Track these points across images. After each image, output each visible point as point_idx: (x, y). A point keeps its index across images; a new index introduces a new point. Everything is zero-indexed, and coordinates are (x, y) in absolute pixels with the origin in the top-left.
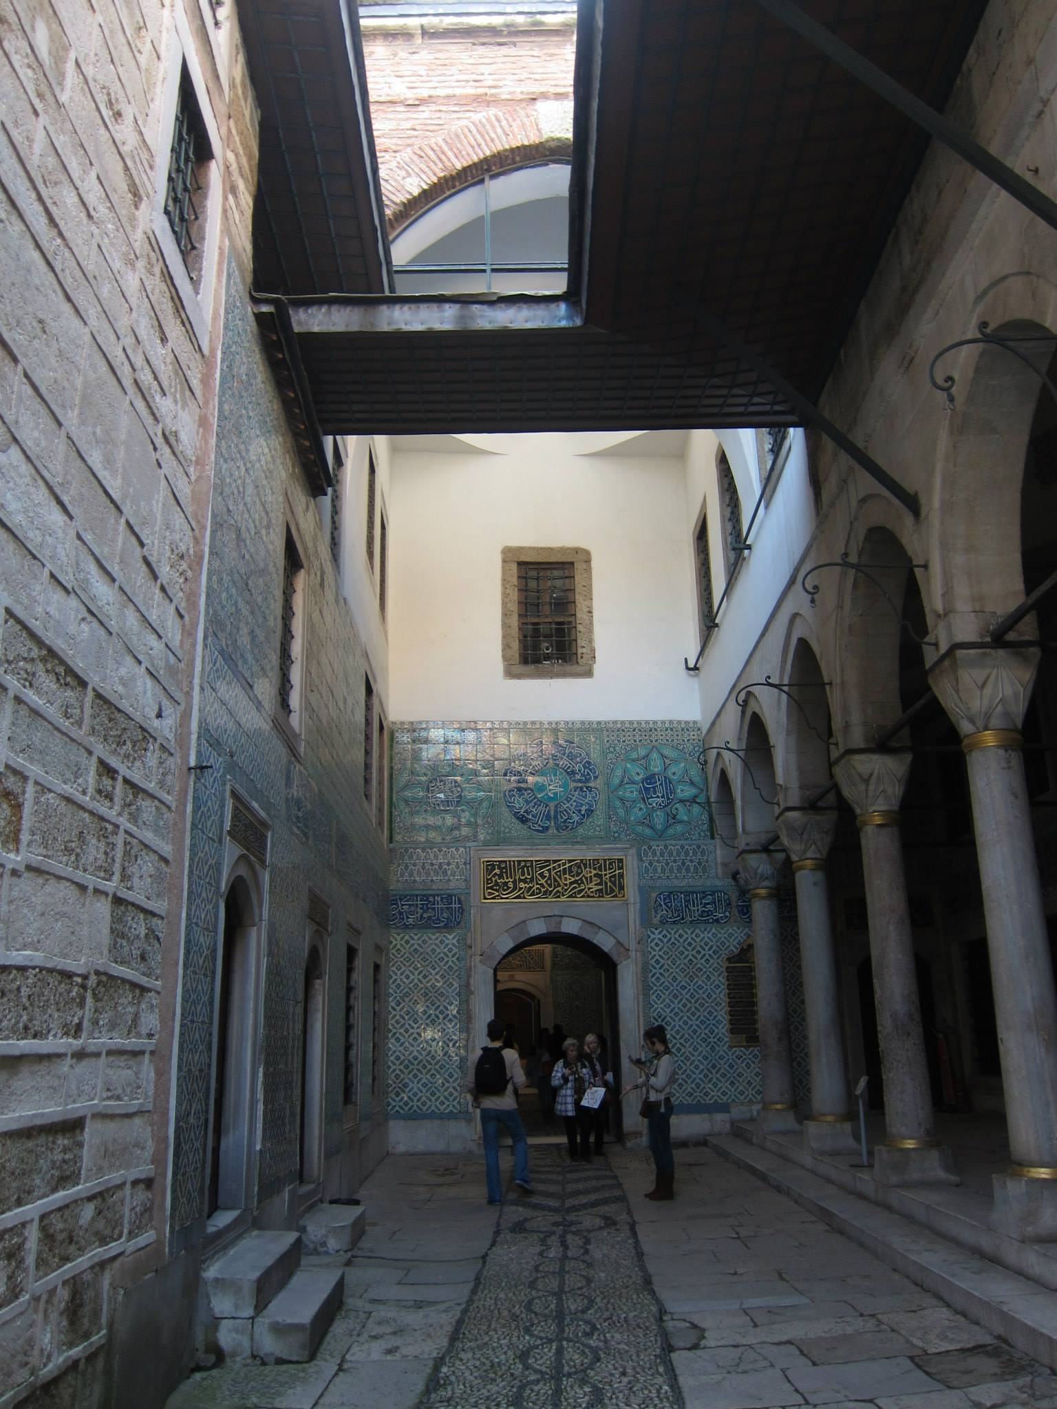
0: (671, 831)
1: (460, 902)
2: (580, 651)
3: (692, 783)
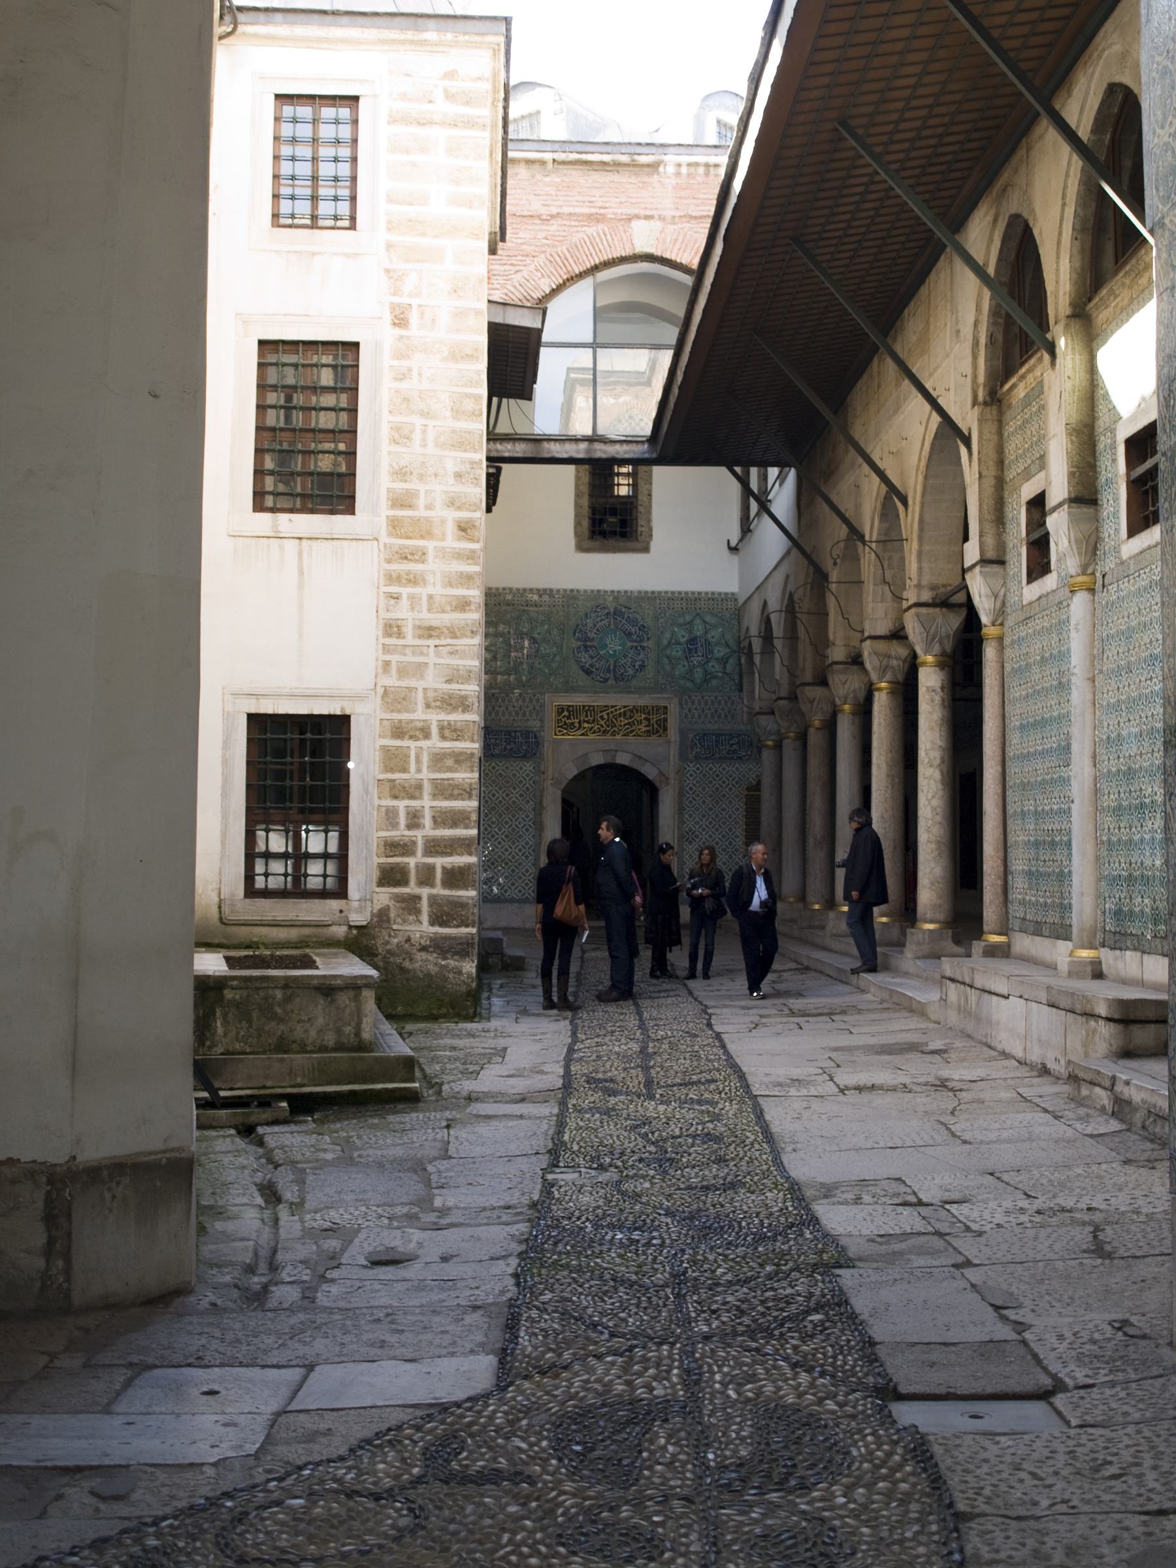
1: (536, 737)
2: (640, 529)
3: (727, 645)
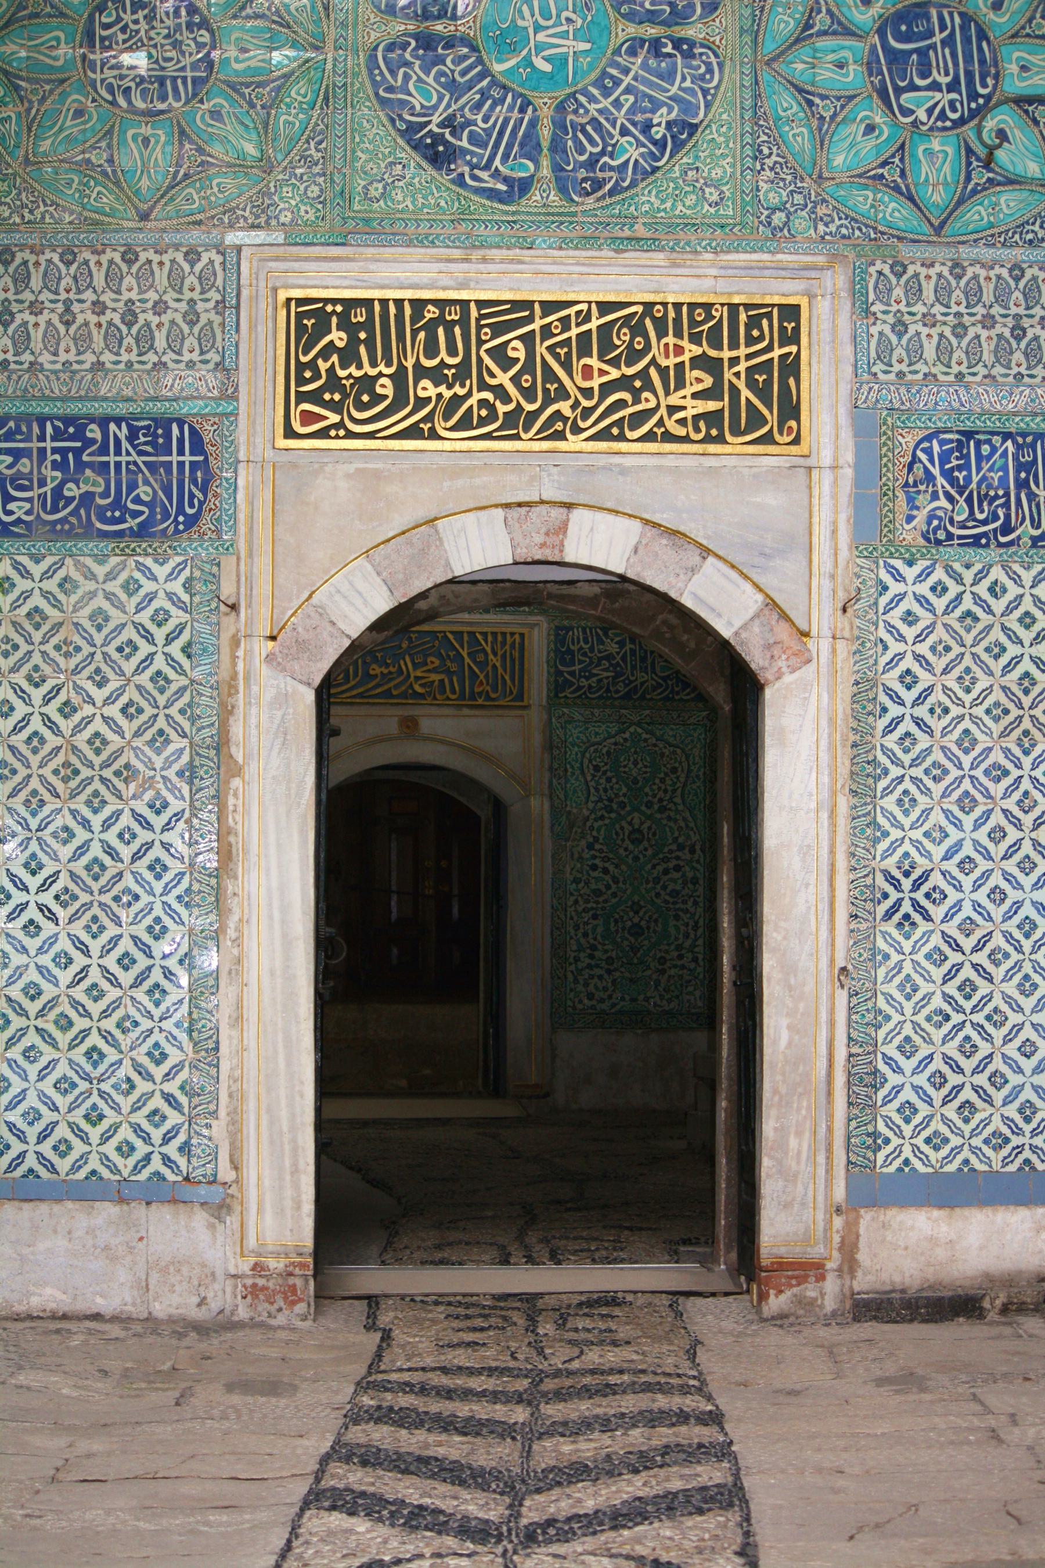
0: (977, 214)
1: (198, 445)
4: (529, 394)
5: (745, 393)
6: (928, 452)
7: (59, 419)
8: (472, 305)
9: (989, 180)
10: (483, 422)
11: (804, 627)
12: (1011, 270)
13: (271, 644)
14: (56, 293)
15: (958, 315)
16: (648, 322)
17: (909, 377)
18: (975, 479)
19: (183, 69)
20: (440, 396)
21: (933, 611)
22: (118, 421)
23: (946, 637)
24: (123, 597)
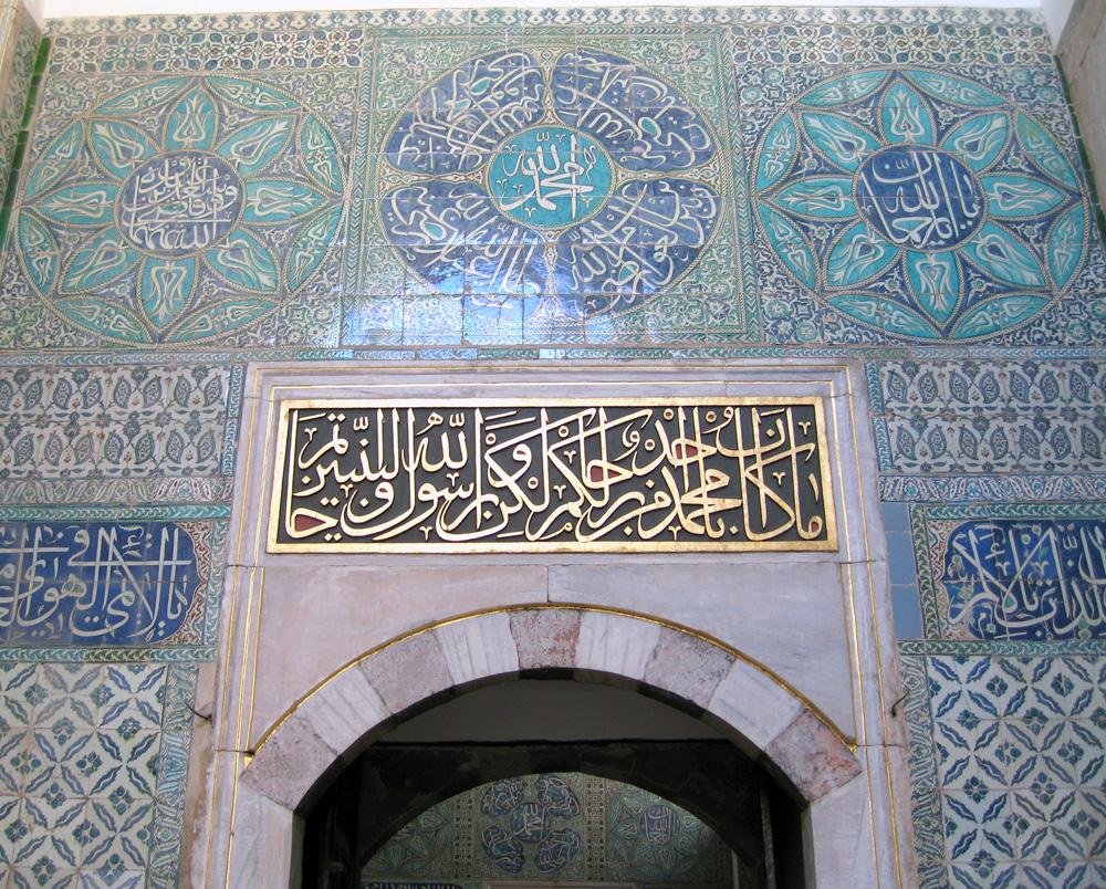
0: (981, 317)
3: (1038, 175)
4: (536, 495)
5: (764, 490)
6: (966, 543)
7: (49, 524)
8: (478, 412)
9: (988, 288)
10: (486, 523)
11: (848, 732)
12: (1024, 368)
13: (248, 759)
14: (65, 408)
15: (977, 409)
16: (659, 425)
17: (935, 469)
18: (1020, 569)
19: (211, 216)
20: (442, 499)
21: (993, 711)
22: (108, 526)
23: (1012, 740)
24: (91, 706)
